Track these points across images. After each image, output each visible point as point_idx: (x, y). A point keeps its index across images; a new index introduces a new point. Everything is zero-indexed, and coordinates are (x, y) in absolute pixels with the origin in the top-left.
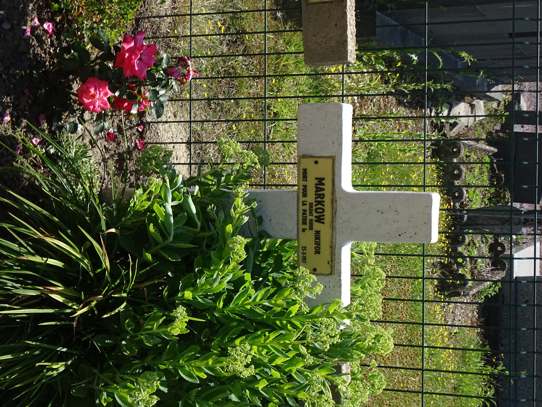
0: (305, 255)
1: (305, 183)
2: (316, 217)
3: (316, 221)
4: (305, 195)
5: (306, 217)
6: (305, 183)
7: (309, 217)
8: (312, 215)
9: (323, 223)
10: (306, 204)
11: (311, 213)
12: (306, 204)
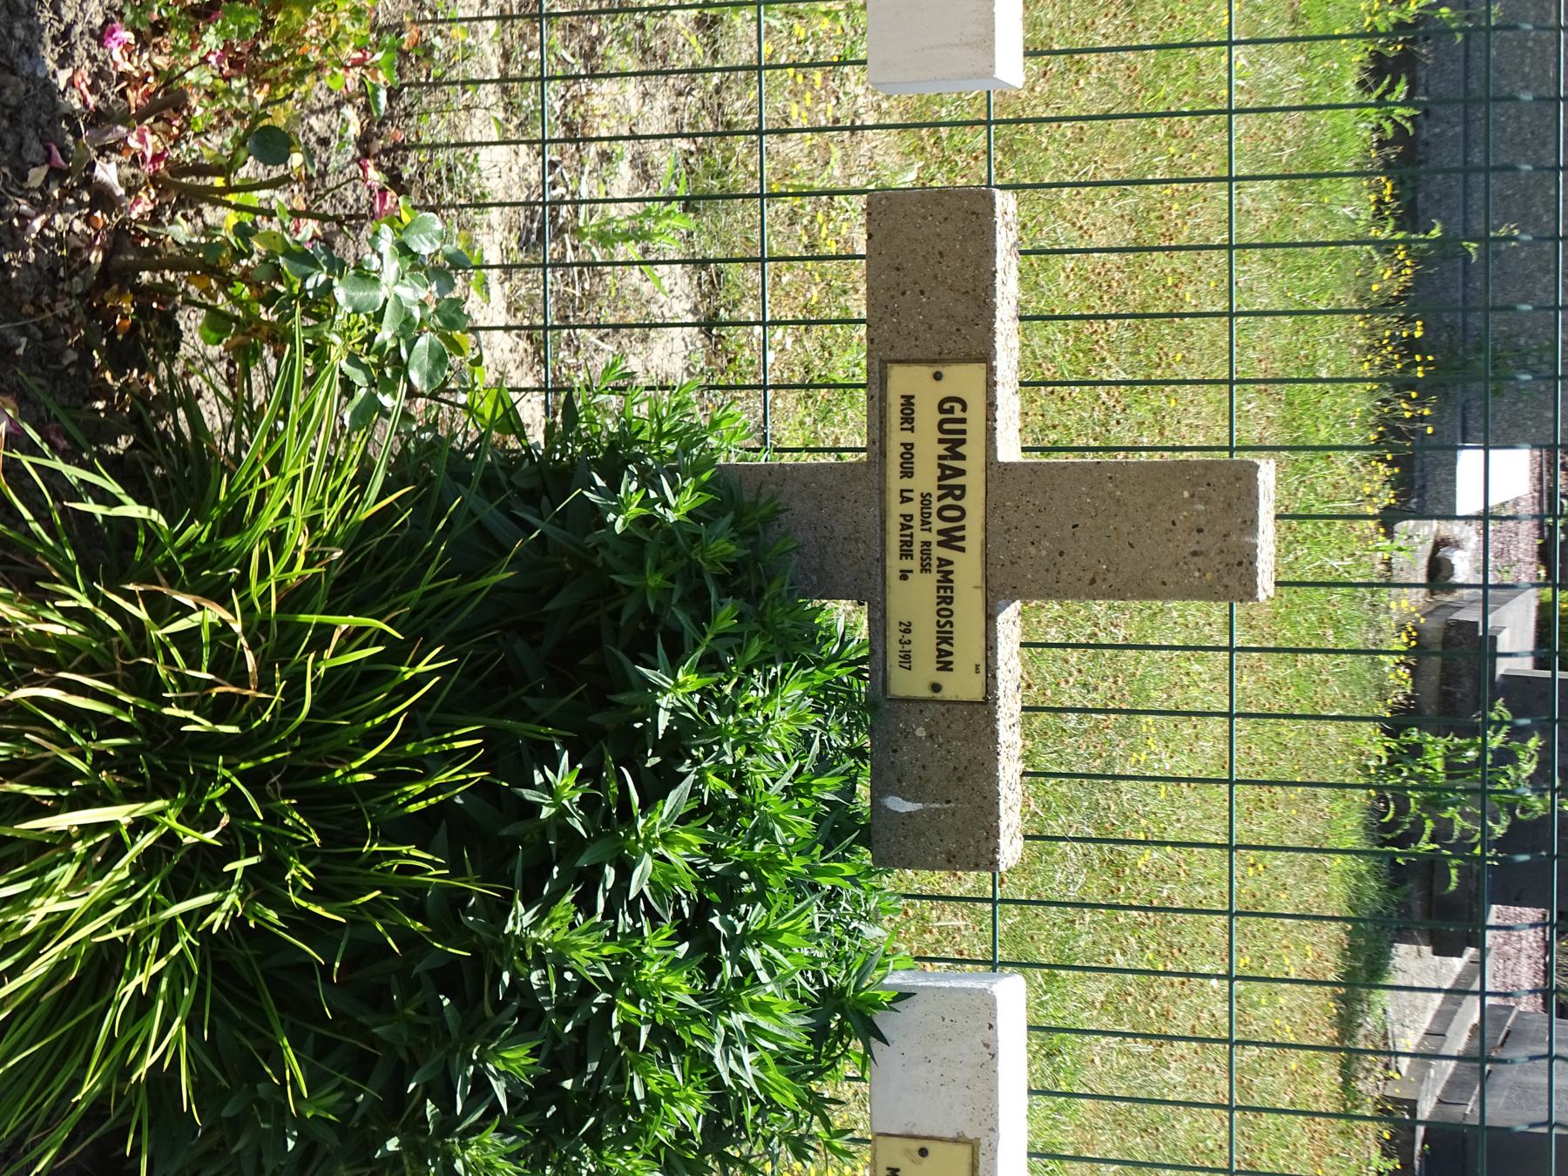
0: (907, 647)
1: (907, 437)
2: (940, 532)
3: (940, 544)
4: (907, 473)
5: (911, 535)
6: (907, 437)
7: (919, 536)
9: (962, 550)
11: (924, 523)
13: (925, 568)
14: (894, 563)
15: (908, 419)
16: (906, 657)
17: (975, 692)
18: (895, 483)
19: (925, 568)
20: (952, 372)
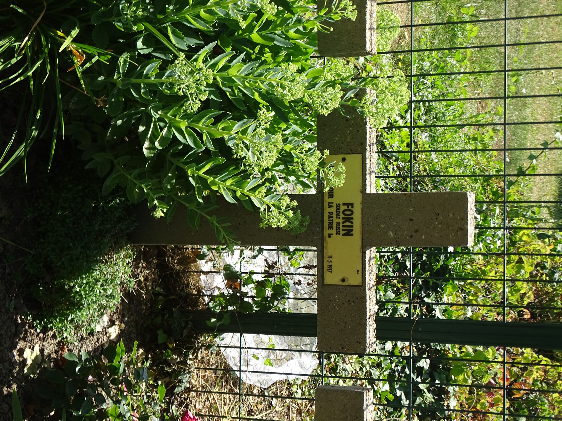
0: (331, 264)
3: (344, 235)
5: (332, 220)
7: (335, 220)
8: (339, 218)
13: (338, 233)
14: (326, 232)
16: (330, 267)
18: (327, 200)
19: (338, 233)
20: (348, 157)
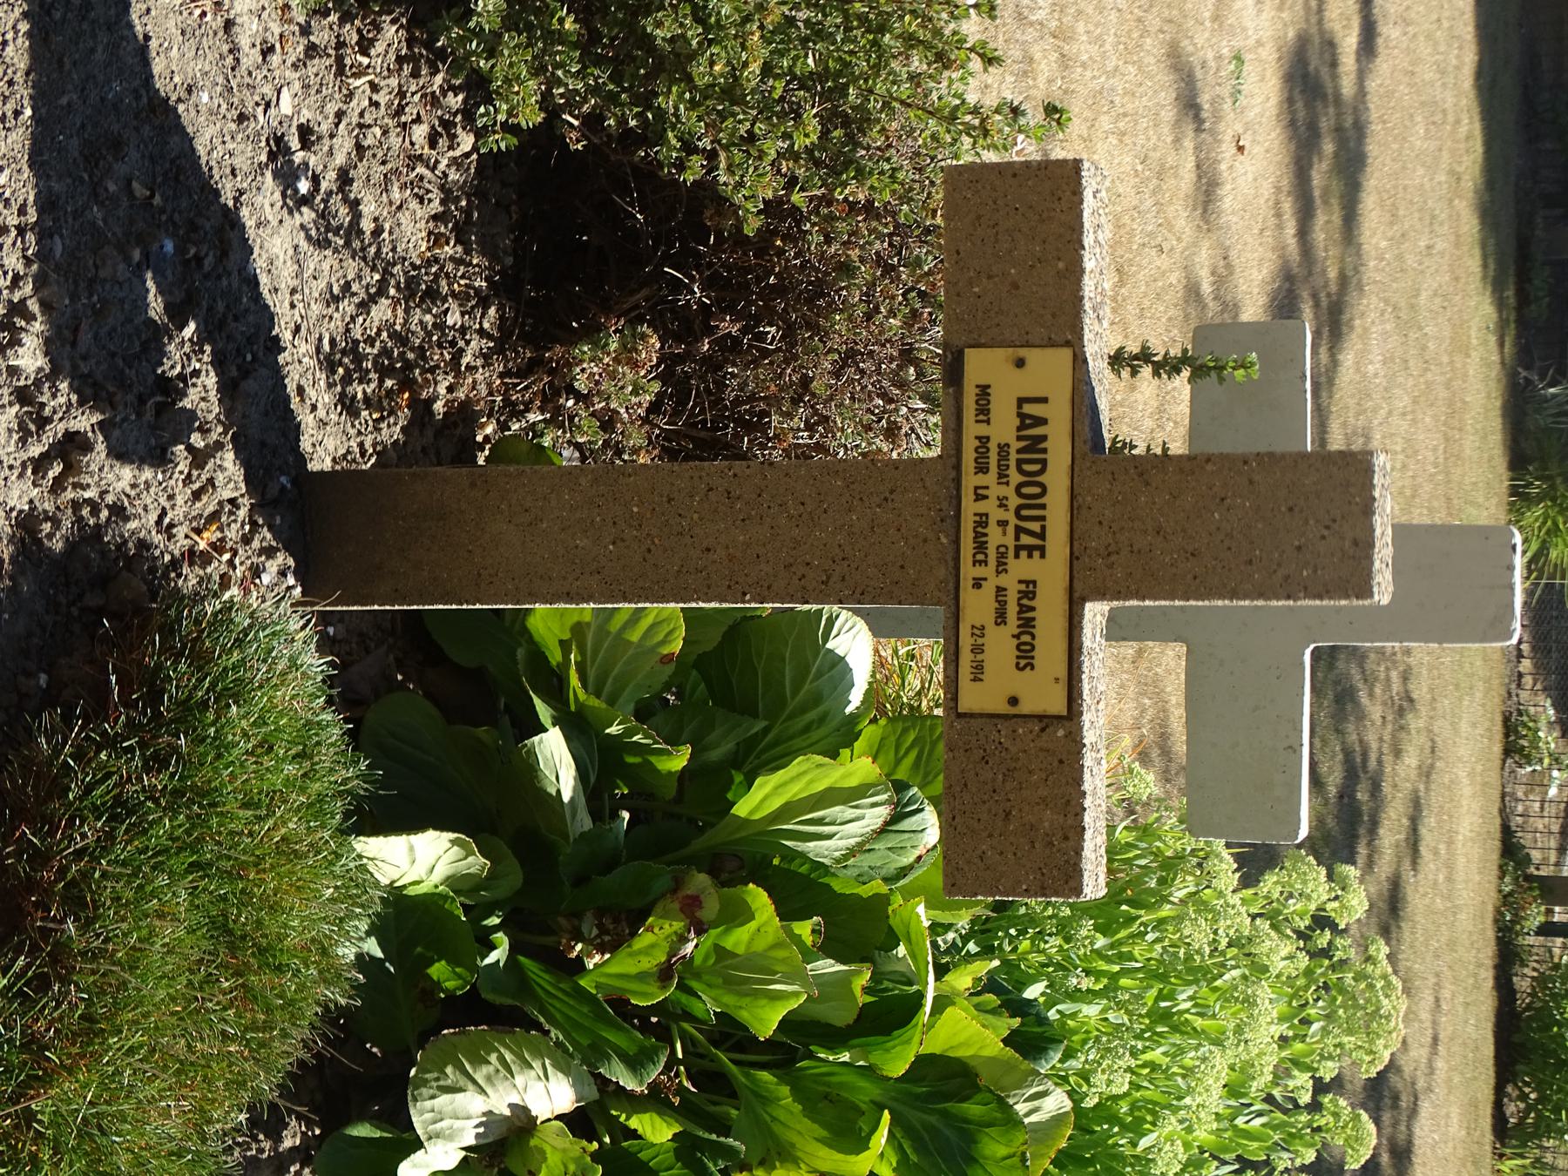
0: (979, 657)
1: (983, 430)
6: (983, 430)
7: (995, 537)
10: (986, 497)
12: (986, 497)
15: (983, 411)
17: (1058, 706)
18: (970, 480)
20: (1032, 355)
